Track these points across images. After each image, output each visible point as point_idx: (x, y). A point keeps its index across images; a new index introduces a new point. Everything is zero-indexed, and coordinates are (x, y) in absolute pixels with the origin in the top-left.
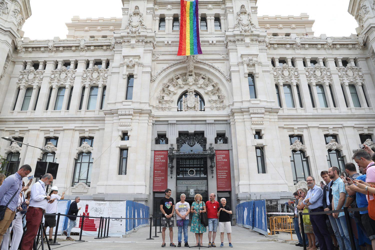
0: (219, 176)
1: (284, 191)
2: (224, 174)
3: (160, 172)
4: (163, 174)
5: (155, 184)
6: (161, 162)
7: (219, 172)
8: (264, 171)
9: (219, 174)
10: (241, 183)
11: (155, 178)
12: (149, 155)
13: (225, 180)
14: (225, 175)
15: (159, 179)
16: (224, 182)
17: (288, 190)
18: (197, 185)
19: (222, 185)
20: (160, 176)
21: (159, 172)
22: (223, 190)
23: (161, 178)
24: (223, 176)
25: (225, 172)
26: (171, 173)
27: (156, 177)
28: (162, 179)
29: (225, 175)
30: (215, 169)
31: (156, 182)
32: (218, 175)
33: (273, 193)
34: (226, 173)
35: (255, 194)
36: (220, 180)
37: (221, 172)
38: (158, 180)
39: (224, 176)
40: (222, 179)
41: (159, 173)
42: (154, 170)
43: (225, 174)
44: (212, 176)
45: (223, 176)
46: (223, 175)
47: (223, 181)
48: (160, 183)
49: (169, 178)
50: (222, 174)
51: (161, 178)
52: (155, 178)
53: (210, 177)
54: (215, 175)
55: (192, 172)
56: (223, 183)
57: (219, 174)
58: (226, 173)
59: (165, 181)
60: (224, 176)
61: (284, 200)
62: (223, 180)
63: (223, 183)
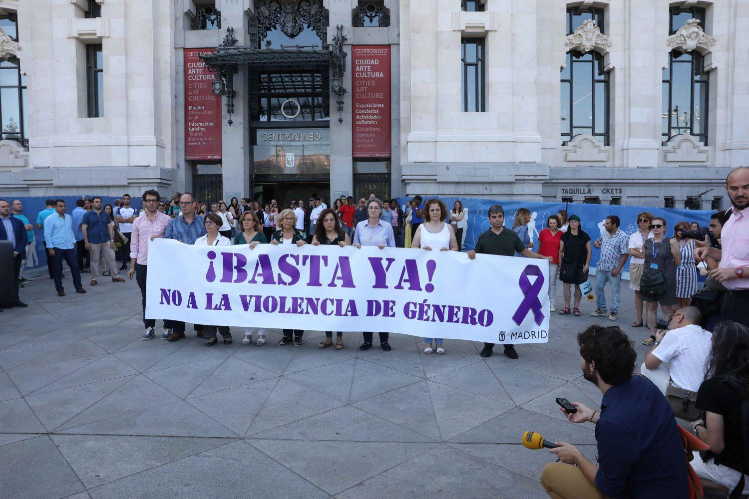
0: (358, 120)
1: (528, 161)
2: (373, 114)
3: (203, 108)
4: (210, 113)
5: (191, 142)
6: (202, 81)
7: (360, 109)
8: (482, 106)
9: (360, 115)
10: (413, 136)
11: (190, 124)
12: (169, 59)
13: (375, 129)
14: (376, 117)
15: (199, 127)
16: (373, 135)
17: (538, 159)
18: (305, 143)
19: (365, 143)
20: (202, 118)
21: (200, 108)
22: (368, 156)
23: (204, 124)
24: (371, 120)
25: (375, 109)
26: (231, 110)
27: (192, 121)
28: (207, 127)
29: (376, 117)
30: (348, 100)
31: (193, 134)
32: (358, 117)
33: (496, 165)
34: (377, 111)
35: (448, 168)
36: (362, 129)
37: (364, 109)
38: (196, 129)
39: (374, 120)
40: (368, 125)
41: (200, 110)
42: (187, 103)
43: (377, 114)
44: (338, 117)
45: (371, 120)
46: (370, 117)
47: (369, 132)
48: (204, 139)
49: (225, 122)
50: (369, 114)
51: (204, 124)
52: (190, 124)
53: (333, 118)
54: (347, 116)
55: (291, 108)
56: (370, 138)
57: (360, 115)
58: (377, 111)
59: (216, 132)
60: (374, 120)
61: (525, 185)
62: (371, 129)
63: (370, 138)
